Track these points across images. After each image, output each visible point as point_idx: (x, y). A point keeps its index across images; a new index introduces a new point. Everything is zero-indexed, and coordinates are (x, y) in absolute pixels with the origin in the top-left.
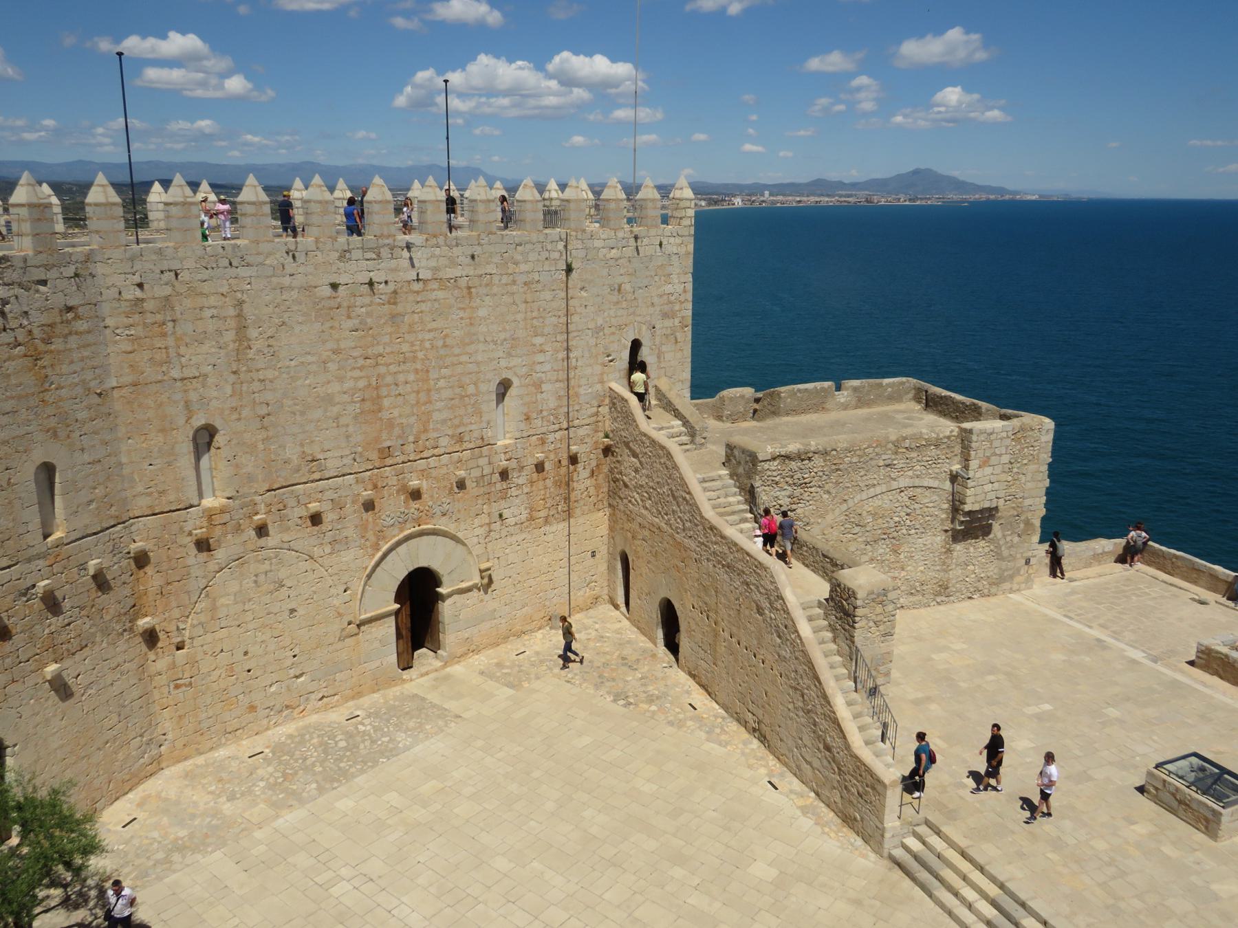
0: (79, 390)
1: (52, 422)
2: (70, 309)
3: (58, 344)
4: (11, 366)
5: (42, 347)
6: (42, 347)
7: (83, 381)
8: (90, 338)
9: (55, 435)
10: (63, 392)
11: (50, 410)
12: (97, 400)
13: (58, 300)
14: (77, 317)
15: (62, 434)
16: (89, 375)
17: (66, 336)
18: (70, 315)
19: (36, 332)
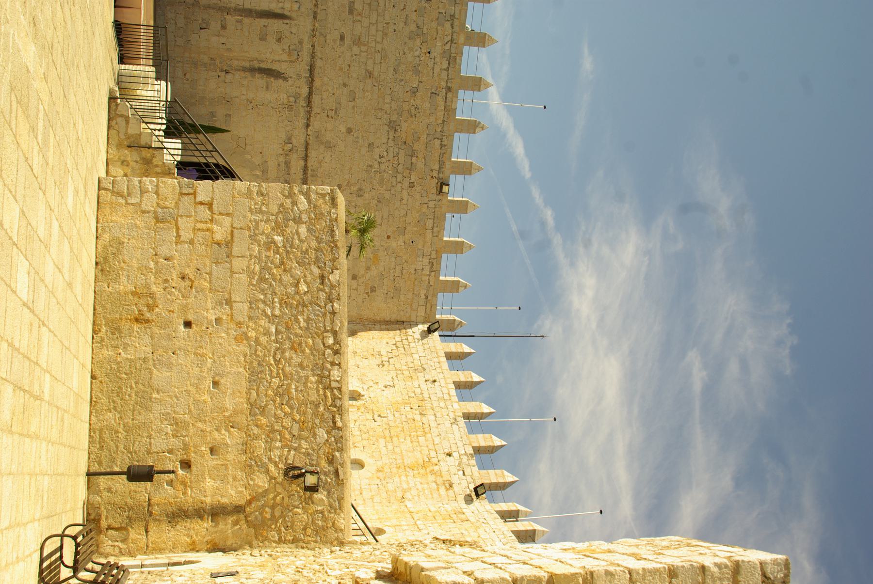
0: (405, 486)
1: (387, 470)
2: (451, 486)
3: (431, 478)
4: (418, 455)
5: (428, 470)
6: (428, 470)
7: (410, 489)
8: (435, 495)
9: (379, 471)
10: (403, 478)
11: (394, 470)
12: (400, 494)
13: (455, 480)
14: (447, 489)
15: (380, 474)
16: (414, 492)
17: (436, 482)
18: (447, 485)
19: (436, 468)
